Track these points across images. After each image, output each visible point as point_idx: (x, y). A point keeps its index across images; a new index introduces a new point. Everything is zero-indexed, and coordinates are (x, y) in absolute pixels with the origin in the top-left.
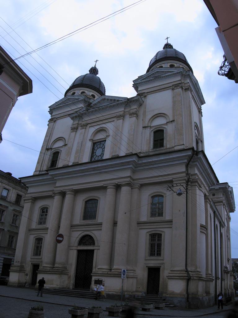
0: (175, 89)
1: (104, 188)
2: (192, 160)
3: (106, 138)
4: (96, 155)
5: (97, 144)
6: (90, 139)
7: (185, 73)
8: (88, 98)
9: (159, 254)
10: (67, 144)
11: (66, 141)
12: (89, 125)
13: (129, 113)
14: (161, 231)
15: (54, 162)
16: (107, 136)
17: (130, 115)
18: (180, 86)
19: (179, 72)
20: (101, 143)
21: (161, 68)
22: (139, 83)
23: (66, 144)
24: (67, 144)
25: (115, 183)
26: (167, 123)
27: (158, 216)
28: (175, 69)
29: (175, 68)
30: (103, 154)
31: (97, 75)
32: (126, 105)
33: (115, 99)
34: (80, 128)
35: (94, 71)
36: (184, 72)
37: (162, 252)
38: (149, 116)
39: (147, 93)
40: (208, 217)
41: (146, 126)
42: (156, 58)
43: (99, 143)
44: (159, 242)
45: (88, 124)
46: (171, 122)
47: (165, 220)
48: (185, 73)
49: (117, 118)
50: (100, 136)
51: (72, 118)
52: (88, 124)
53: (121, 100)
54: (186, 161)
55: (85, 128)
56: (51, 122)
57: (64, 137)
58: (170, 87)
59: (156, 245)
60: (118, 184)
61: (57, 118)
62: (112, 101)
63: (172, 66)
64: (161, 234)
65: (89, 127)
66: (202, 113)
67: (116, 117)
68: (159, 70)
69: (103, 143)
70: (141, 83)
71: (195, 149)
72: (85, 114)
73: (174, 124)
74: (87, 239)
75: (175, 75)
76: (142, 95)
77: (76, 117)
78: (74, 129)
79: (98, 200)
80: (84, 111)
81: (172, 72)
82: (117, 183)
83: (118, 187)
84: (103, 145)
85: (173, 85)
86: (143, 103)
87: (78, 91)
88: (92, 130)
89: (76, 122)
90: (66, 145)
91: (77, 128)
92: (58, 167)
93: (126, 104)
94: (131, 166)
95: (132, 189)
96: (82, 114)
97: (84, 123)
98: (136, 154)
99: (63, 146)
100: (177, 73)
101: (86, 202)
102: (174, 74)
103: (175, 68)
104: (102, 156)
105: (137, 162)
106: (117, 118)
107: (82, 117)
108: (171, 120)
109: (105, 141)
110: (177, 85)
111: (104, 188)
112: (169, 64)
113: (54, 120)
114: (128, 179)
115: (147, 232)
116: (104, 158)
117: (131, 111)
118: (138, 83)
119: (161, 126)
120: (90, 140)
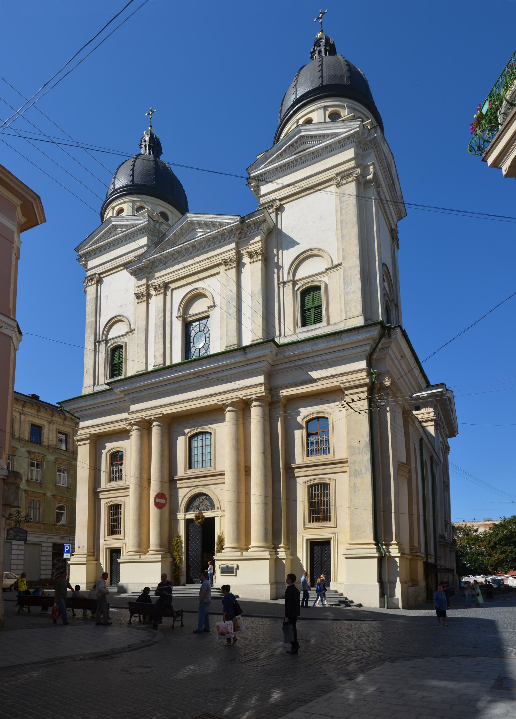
10: (134, 330)
11: (132, 322)
12: (172, 286)
13: (247, 252)
20: (202, 322)
23: (132, 328)
24: (134, 330)
25: (239, 397)
28: (343, 124)
39: (281, 200)
40: (411, 447)
43: (198, 323)
47: (334, 459)
51: (134, 273)
53: (228, 224)
57: (125, 315)
63: (334, 117)
73: (339, 272)
75: (340, 145)
76: (270, 207)
78: (143, 297)
90: (132, 331)
91: (149, 296)
103: (343, 121)
104: (206, 348)
108: (336, 263)
110: (345, 173)
116: (212, 352)
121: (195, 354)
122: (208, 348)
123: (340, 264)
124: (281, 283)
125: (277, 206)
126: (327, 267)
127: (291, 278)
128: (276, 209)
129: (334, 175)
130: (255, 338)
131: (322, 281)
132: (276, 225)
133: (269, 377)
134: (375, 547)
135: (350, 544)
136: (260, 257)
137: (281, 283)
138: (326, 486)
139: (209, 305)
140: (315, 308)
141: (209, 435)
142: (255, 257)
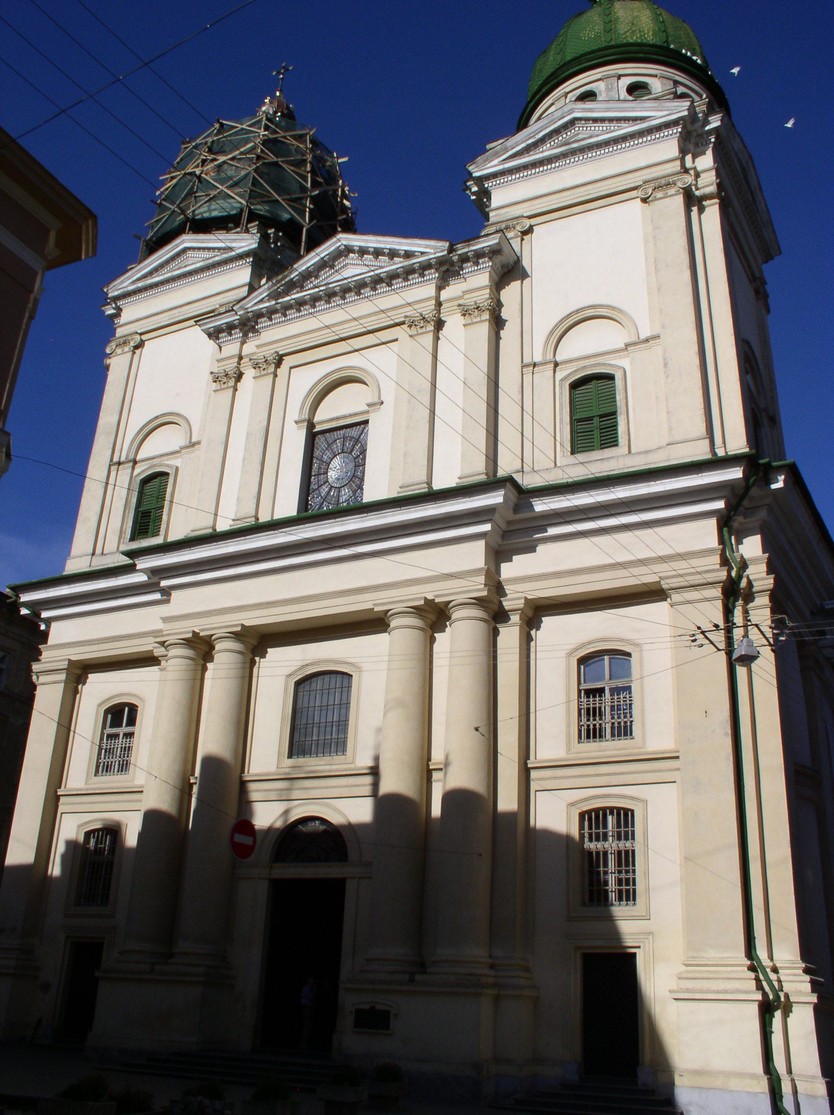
0: (656, 199)
2: (746, 503)
4: (327, 481)
6: (297, 418)
14: (632, 798)
16: (369, 405)
17: (464, 315)
18: (680, 184)
19: (675, 123)
21: (588, 105)
22: (494, 175)
26: (627, 345)
27: (613, 735)
29: (656, 99)
30: (356, 479)
32: (444, 272)
33: (397, 247)
34: (249, 373)
37: (640, 887)
38: (543, 322)
39: (530, 217)
41: (538, 358)
44: (623, 845)
46: (647, 340)
49: (410, 326)
50: (339, 407)
53: (422, 253)
54: (720, 505)
58: (635, 188)
60: (437, 600)
61: (141, 334)
63: (637, 89)
64: (632, 811)
65: (291, 368)
67: (403, 323)
68: (584, 110)
69: (354, 432)
70: (503, 173)
72: (271, 313)
73: (655, 352)
77: (230, 328)
80: (261, 301)
81: (642, 119)
82: (430, 597)
84: (357, 441)
88: (303, 381)
89: (231, 348)
92: (170, 539)
93: (444, 268)
96: (259, 315)
97: (269, 352)
99: (182, 448)
100: (667, 125)
102: (650, 131)
103: (656, 99)
106: (410, 326)
108: (644, 334)
109: (366, 422)
111: (373, 623)
112: (626, 82)
113: (132, 344)
115: (572, 804)
116: (369, 495)
117: (466, 297)
118: (488, 177)
119: (600, 360)
120: (296, 422)
122: (360, 487)
123: (656, 337)
124: (527, 366)
126: (627, 341)
127: (550, 357)
128: (521, 232)
130: (468, 472)
131: (619, 367)
132: (518, 261)
133: (499, 554)
135: (687, 965)
136: (486, 316)
137: (527, 366)
138: (625, 816)
139: (370, 401)
140: (601, 416)
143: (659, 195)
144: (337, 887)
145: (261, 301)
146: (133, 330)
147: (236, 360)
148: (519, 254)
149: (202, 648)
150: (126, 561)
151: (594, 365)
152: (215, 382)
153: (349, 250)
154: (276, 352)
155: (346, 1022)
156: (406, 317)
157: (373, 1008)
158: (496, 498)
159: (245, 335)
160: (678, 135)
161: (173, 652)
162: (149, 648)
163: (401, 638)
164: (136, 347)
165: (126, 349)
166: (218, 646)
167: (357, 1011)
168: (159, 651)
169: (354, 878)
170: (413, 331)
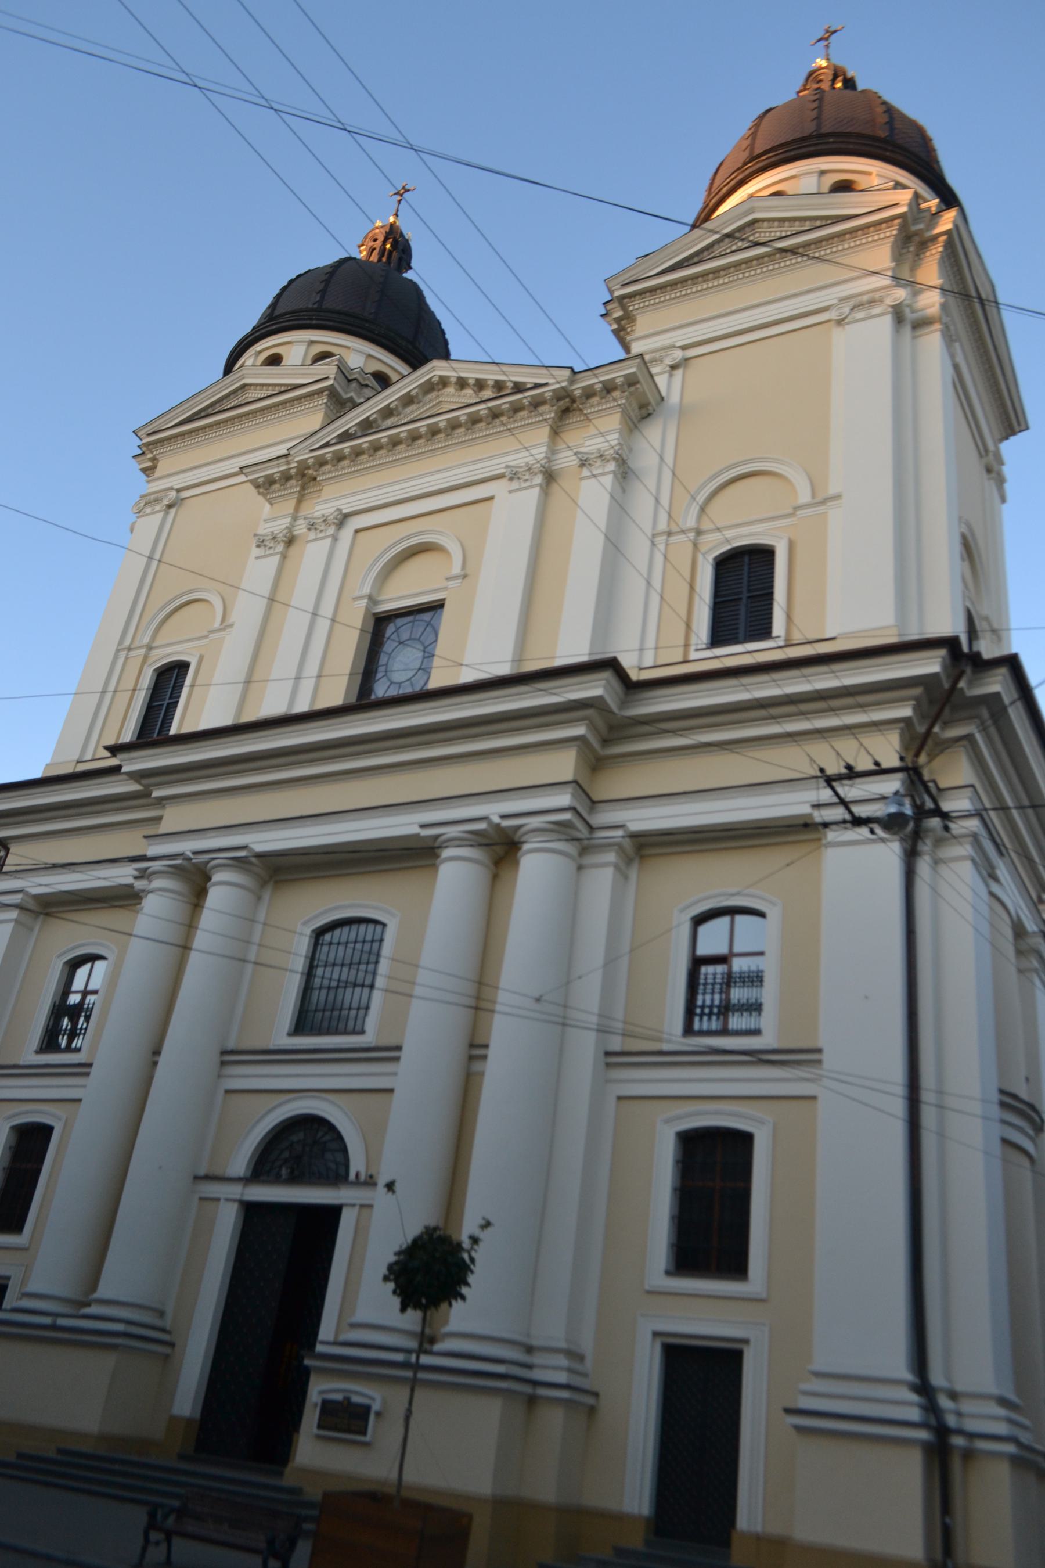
1: (417, 855)
3: (445, 588)
5: (400, 622)
7: (921, 226)
8: (349, 381)
9: (733, 1262)
15: (154, 727)
30: (425, 670)
31: (409, 275)
35: (397, 249)
36: (916, 221)
39: (684, 348)
42: (752, 146)
45: (347, 516)
48: (921, 226)
52: (347, 516)
54: (906, 711)
55: (335, 538)
56: (148, 510)
59: (713, 1201)
61: (178, 491)
62: (488, 393)
65: (357, 531)
66: (1000, 481)
69: (427, 616)
71: (965, 648)
74: (305, 1146)
77: (286, 477)
79: (384, 925)
83: (502, 848)
85: (843, 300)
86: (658, 404)
87: (295, 346)
94: (580, 730)
95: (580, 868)
98: (612, 665)
101: (319, 933)
105: (615, 709)
107: (315, 479)
111: (417, 855)
113: (166, 502)
114: (564, 799)
121: (381, 690)
125: (674, 359)
129: (835, 301)
134: (914, 1397)
136: (611, 466)
141: (379, 928)
142: (598, 464)
143: (860, 315)
144: (332, 1214)
145: (327, 445)
146: (169, 485)
147: (289, 520)
148: (664, 394)
149: (195, 879)
150: (114, 762)
151: (751, 535)
152: (258, 546)
153: (444, 382)
154: (338, 510)
155: (310, 1418)
156: (507, 467)
157: (347, 1399)
158: (594, 687)
159: (303, 488)
160: (892, 239)
161: (158, 883)
162: (129, 880)
163: (457, 875)
164: (170, 506)
165: (158, 508)
166: (217, 877)
167: (325, 1402)
168: (139, 885)
169: (353, 1205)
170: (515, 485)
